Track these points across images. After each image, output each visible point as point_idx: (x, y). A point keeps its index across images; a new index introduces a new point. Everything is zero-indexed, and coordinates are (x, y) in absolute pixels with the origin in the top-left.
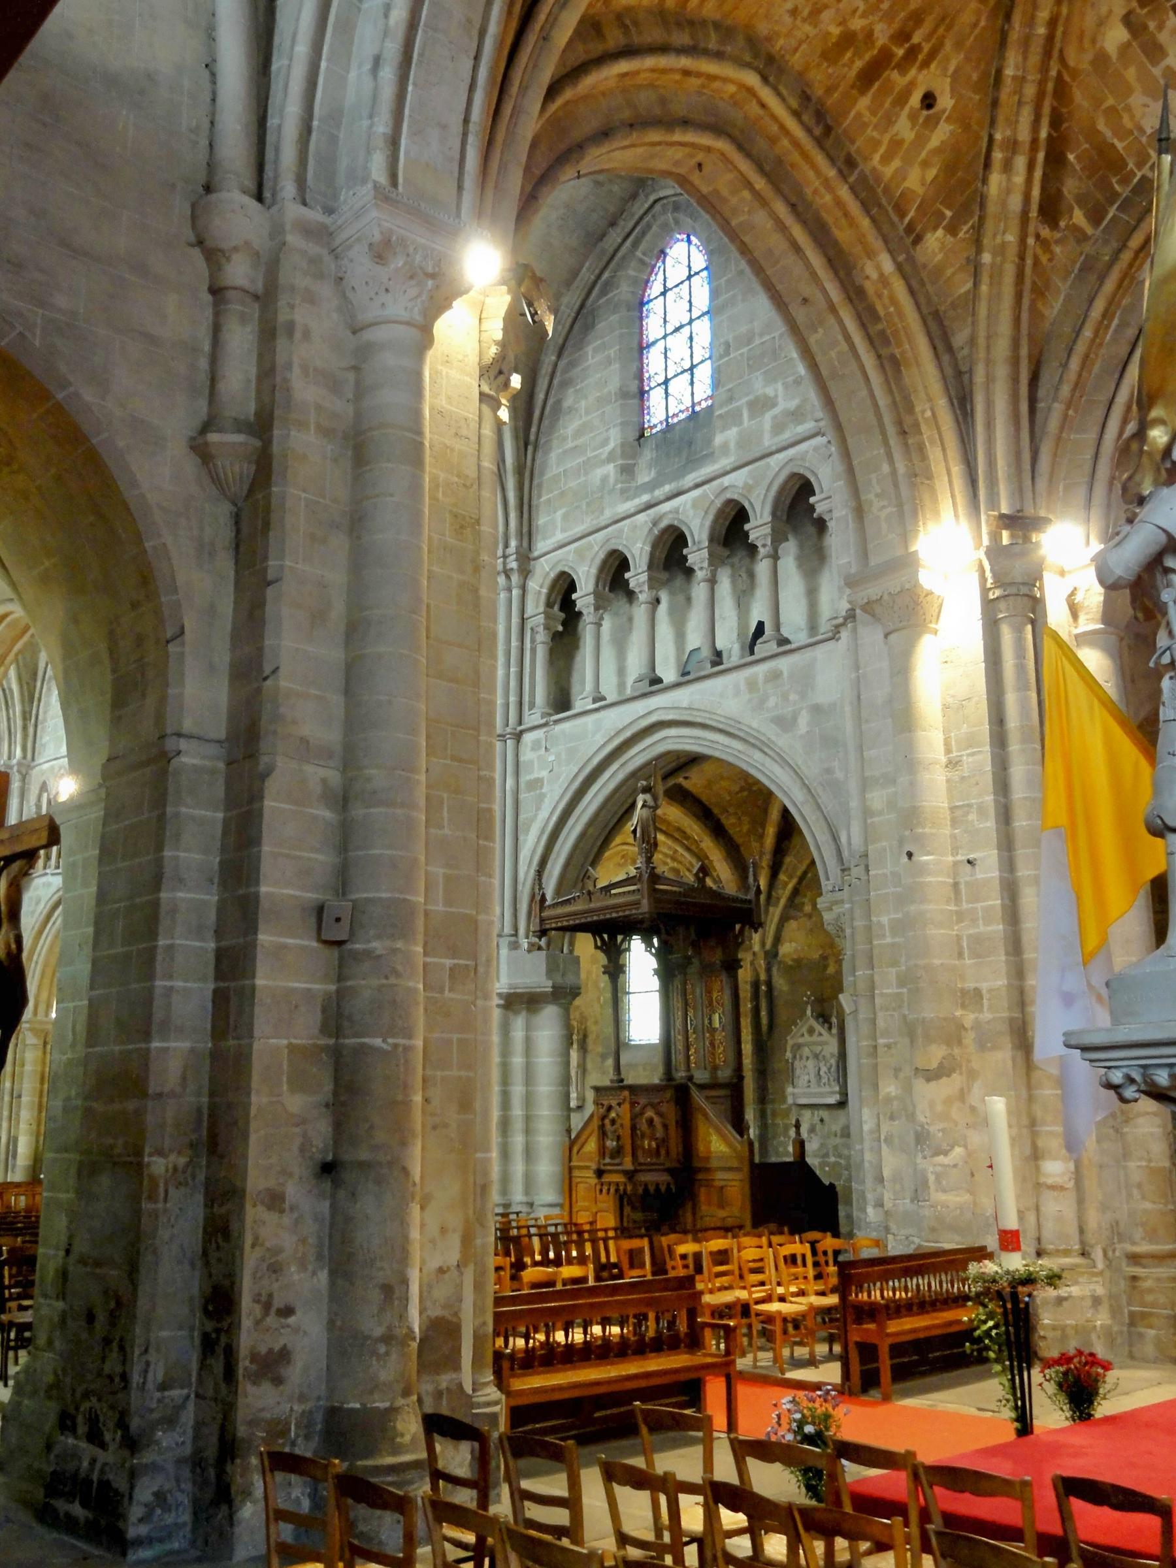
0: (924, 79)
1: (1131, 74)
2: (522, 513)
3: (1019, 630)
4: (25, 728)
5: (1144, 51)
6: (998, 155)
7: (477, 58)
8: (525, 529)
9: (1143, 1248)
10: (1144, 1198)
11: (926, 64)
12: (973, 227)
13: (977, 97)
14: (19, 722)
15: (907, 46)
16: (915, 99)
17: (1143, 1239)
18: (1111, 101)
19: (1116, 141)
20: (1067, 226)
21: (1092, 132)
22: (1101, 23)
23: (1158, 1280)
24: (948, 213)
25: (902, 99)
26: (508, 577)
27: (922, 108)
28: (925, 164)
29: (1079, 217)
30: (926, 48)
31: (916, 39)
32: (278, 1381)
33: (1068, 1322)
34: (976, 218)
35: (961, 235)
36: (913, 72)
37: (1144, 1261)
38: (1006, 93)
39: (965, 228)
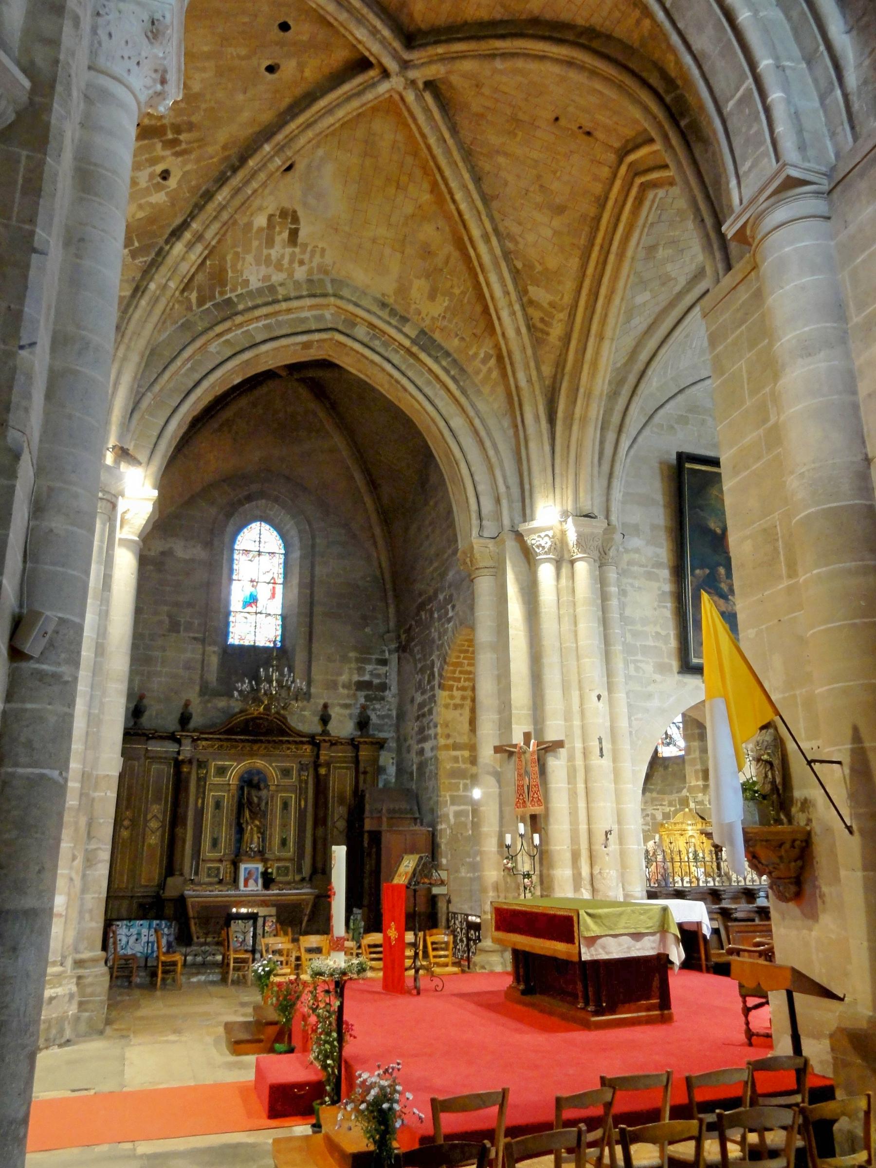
1: (255, 243)
3: (104, 525)
5: (267, 239)
6: (188, 235)
9: (86, 955)
10: (92, 919)
11: (177, 154)
12: (145, 262)
13: (188, 195)
16: (159, 168)
17: (86, 948)
18: (239, 250)
19: (229, 271)
20: (187, 297)
21: (223, 259)
22: (260, 209)
23: (96, 976)
24: (136, 244)
25: (153, 161)
27: (160, 175)
28: (141, 207)
29: (194, 296)
30: (184, 146)
33: (54, 1016)
34: (150, 259)
35: (137, 261)
36: (168, 153)
37: (86, 965)
38: (211, 208)
39: (141, 259)
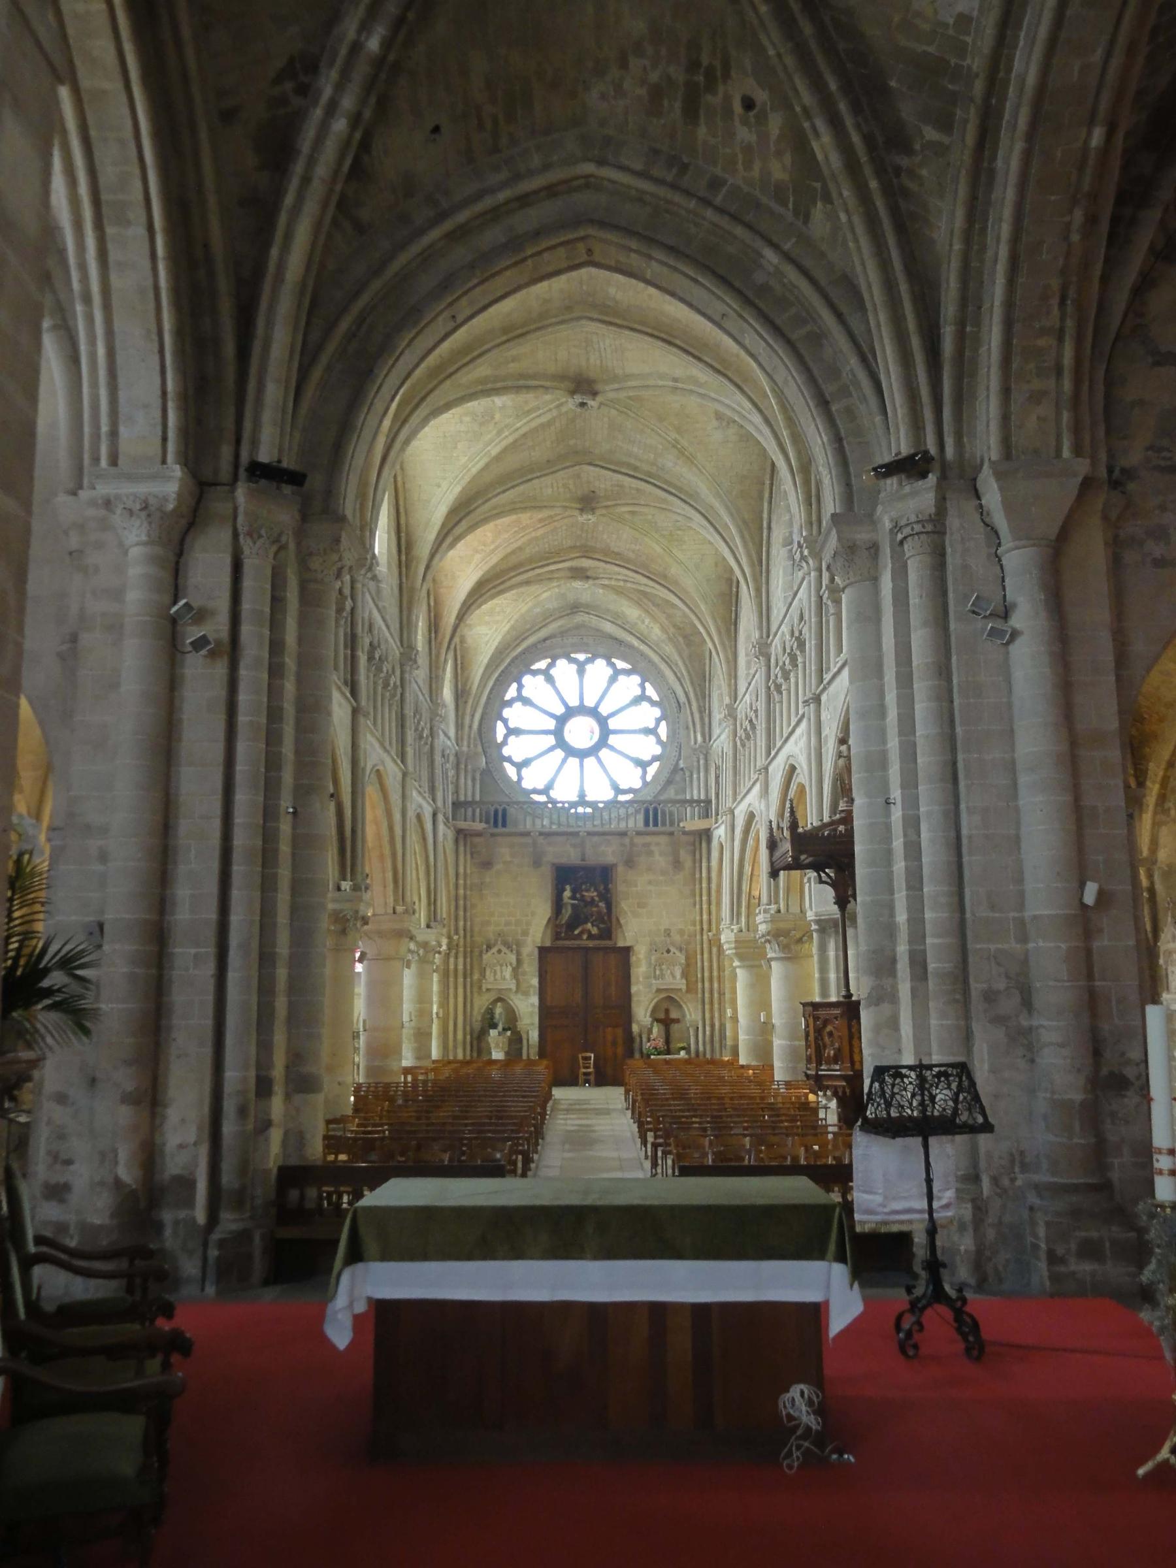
0: (743, 84)
2: (811, 505)
4: (702, 719)
7: (161, 351)
8: (814, 518)
11: (726, 76)
14: (697, 716)
15: (702, 70)
16: (738, 107)
25: (728, 112)
26: (807, 563)
29: (931, 134)
30: (718, 64)
31: (705, 60)
32: (62, 1201)
36: (721, 89)
